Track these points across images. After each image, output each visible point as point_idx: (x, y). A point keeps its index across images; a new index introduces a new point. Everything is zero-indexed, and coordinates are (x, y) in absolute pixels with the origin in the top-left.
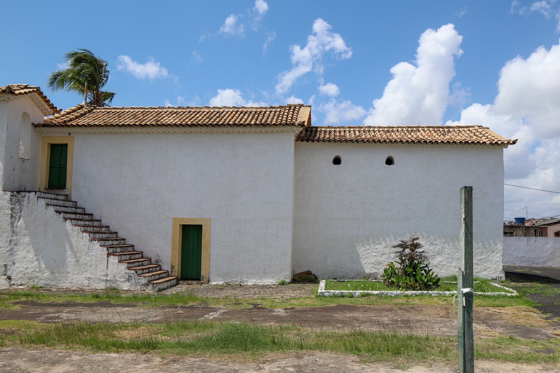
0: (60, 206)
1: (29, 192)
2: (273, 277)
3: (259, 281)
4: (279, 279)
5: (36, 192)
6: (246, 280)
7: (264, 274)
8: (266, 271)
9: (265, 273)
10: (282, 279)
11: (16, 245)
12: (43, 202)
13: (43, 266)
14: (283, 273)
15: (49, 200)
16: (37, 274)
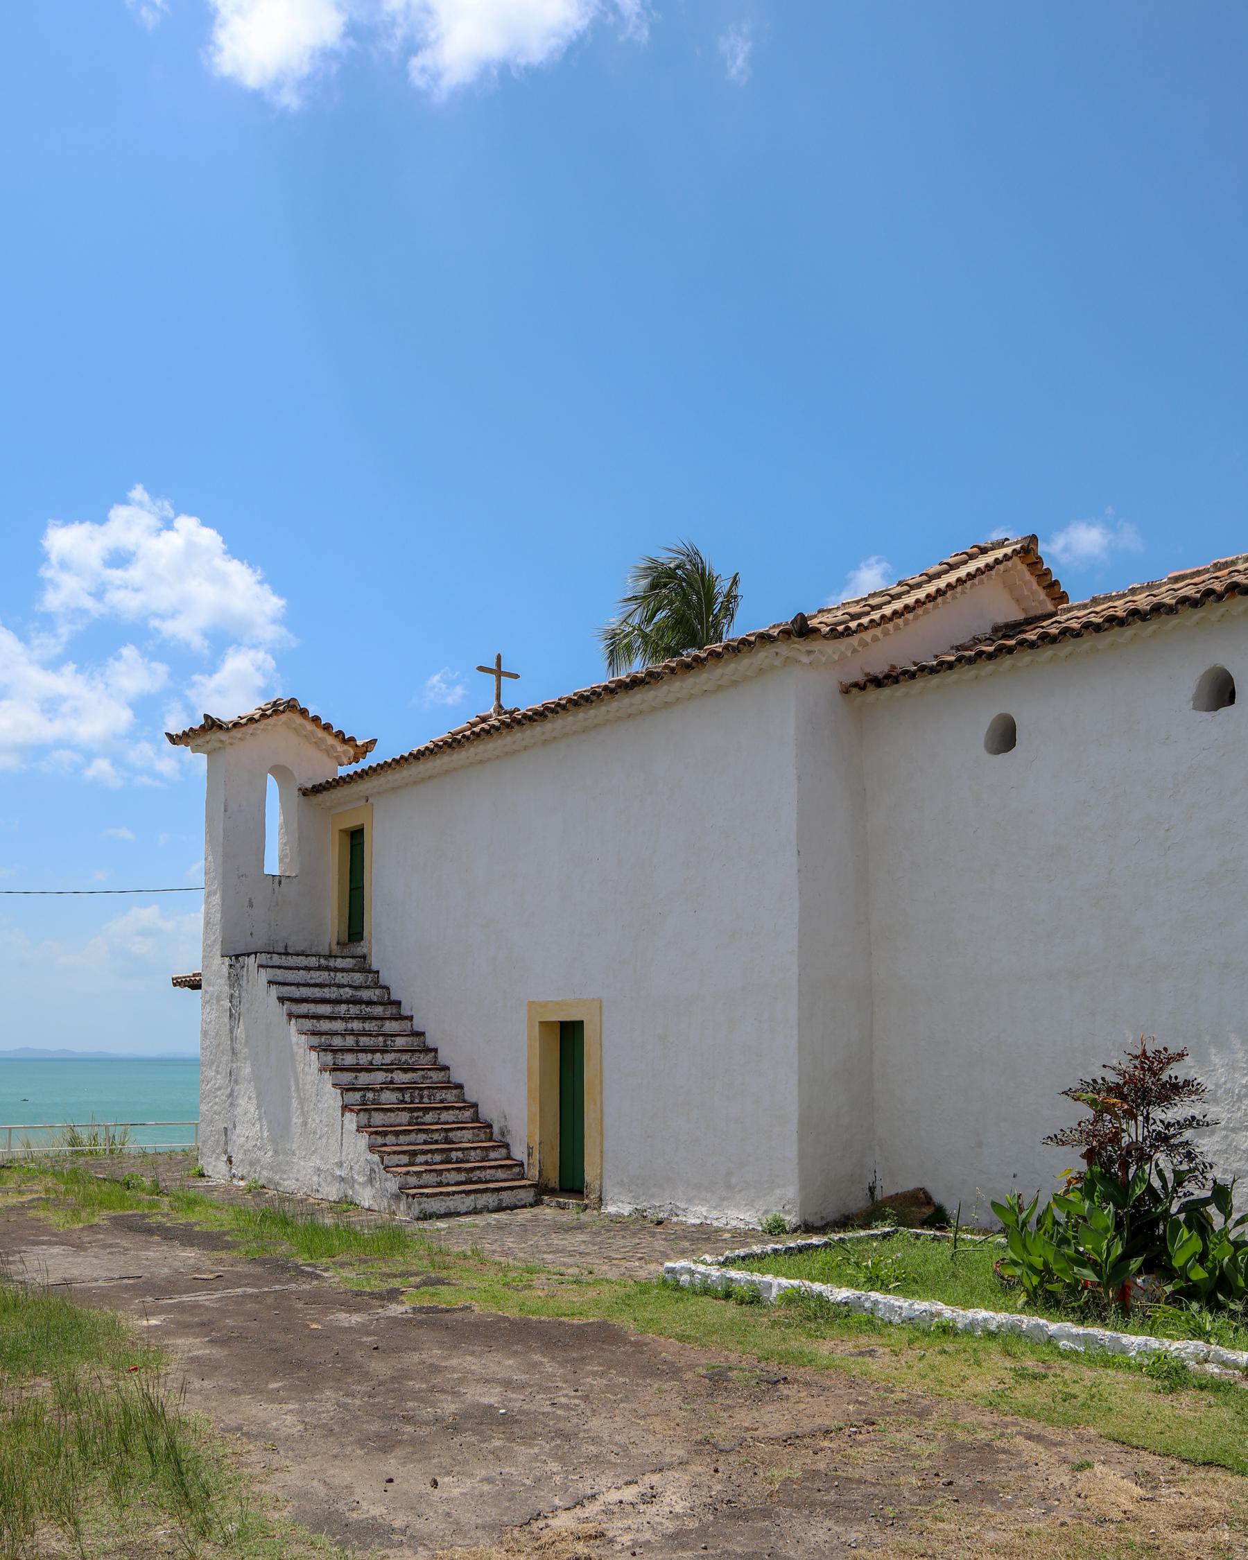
0: (298, 985)
1: (248, 955)
2: (750, 1204)
3: (715, 1214)
4: (766, 1212)
5: (256, 953)
6: (683, 1206)
7: (724, 1188)
8: (734, 1180)
9: (729, 1187)
10: (776, 1212)
11: (236, 1082)
12: (264, 975)
13: (266, 1134)
14: (778, 1192)
15: (279, 972)
16: (258, 1153)
